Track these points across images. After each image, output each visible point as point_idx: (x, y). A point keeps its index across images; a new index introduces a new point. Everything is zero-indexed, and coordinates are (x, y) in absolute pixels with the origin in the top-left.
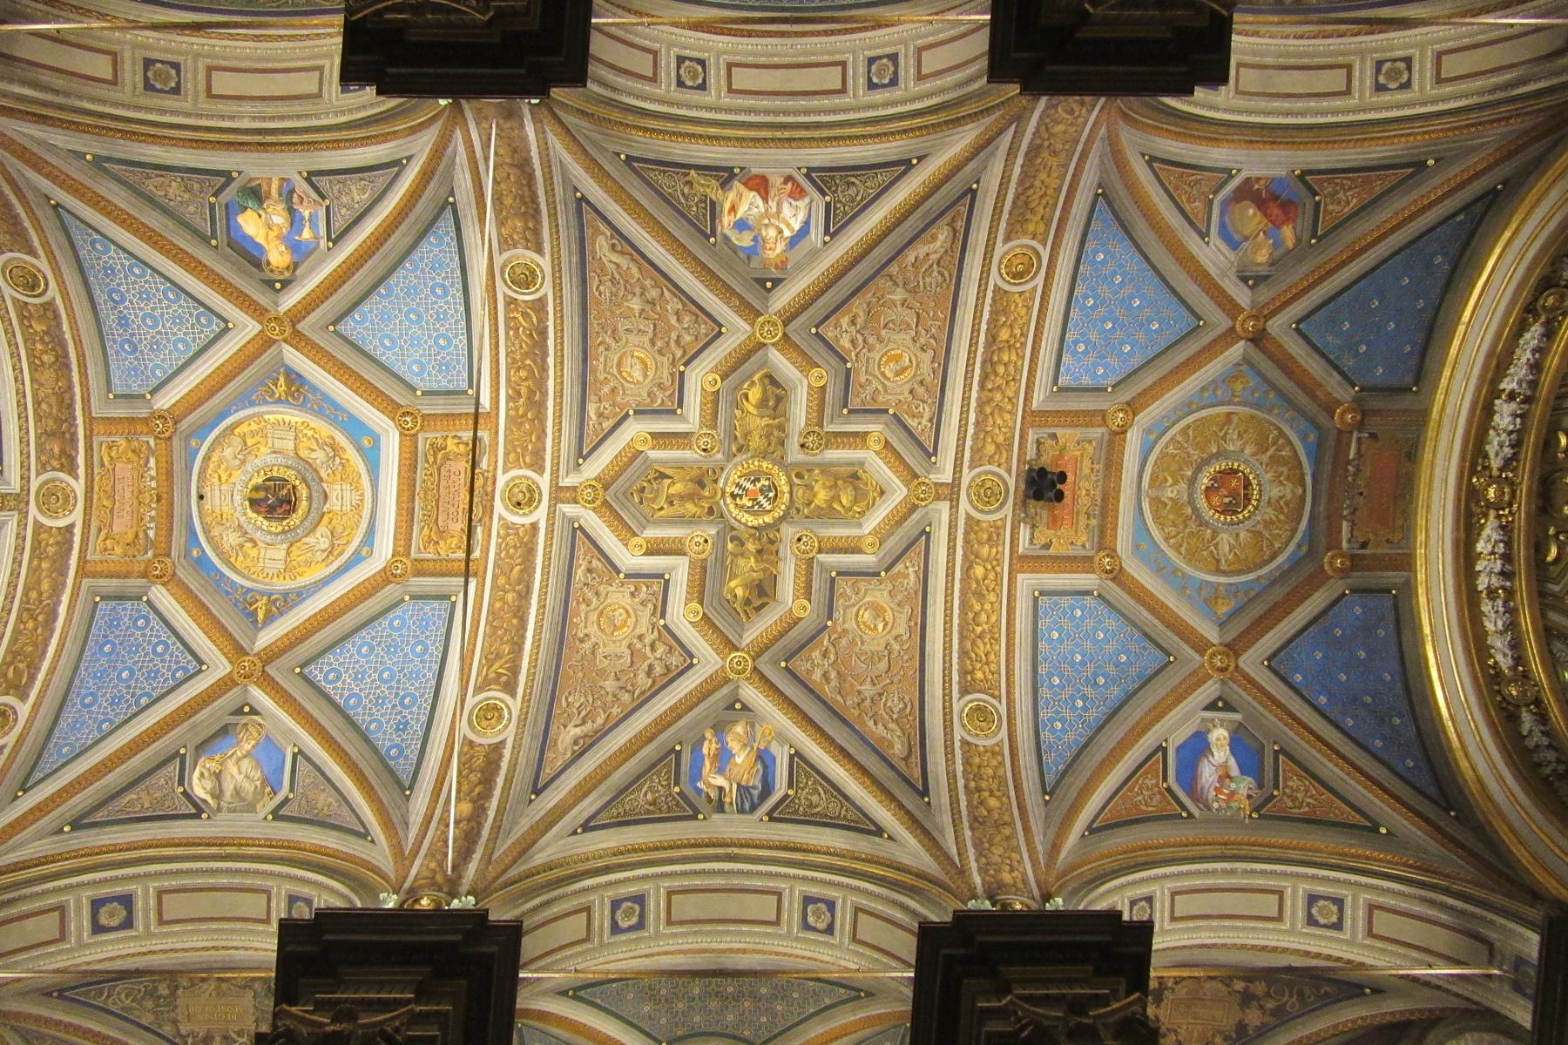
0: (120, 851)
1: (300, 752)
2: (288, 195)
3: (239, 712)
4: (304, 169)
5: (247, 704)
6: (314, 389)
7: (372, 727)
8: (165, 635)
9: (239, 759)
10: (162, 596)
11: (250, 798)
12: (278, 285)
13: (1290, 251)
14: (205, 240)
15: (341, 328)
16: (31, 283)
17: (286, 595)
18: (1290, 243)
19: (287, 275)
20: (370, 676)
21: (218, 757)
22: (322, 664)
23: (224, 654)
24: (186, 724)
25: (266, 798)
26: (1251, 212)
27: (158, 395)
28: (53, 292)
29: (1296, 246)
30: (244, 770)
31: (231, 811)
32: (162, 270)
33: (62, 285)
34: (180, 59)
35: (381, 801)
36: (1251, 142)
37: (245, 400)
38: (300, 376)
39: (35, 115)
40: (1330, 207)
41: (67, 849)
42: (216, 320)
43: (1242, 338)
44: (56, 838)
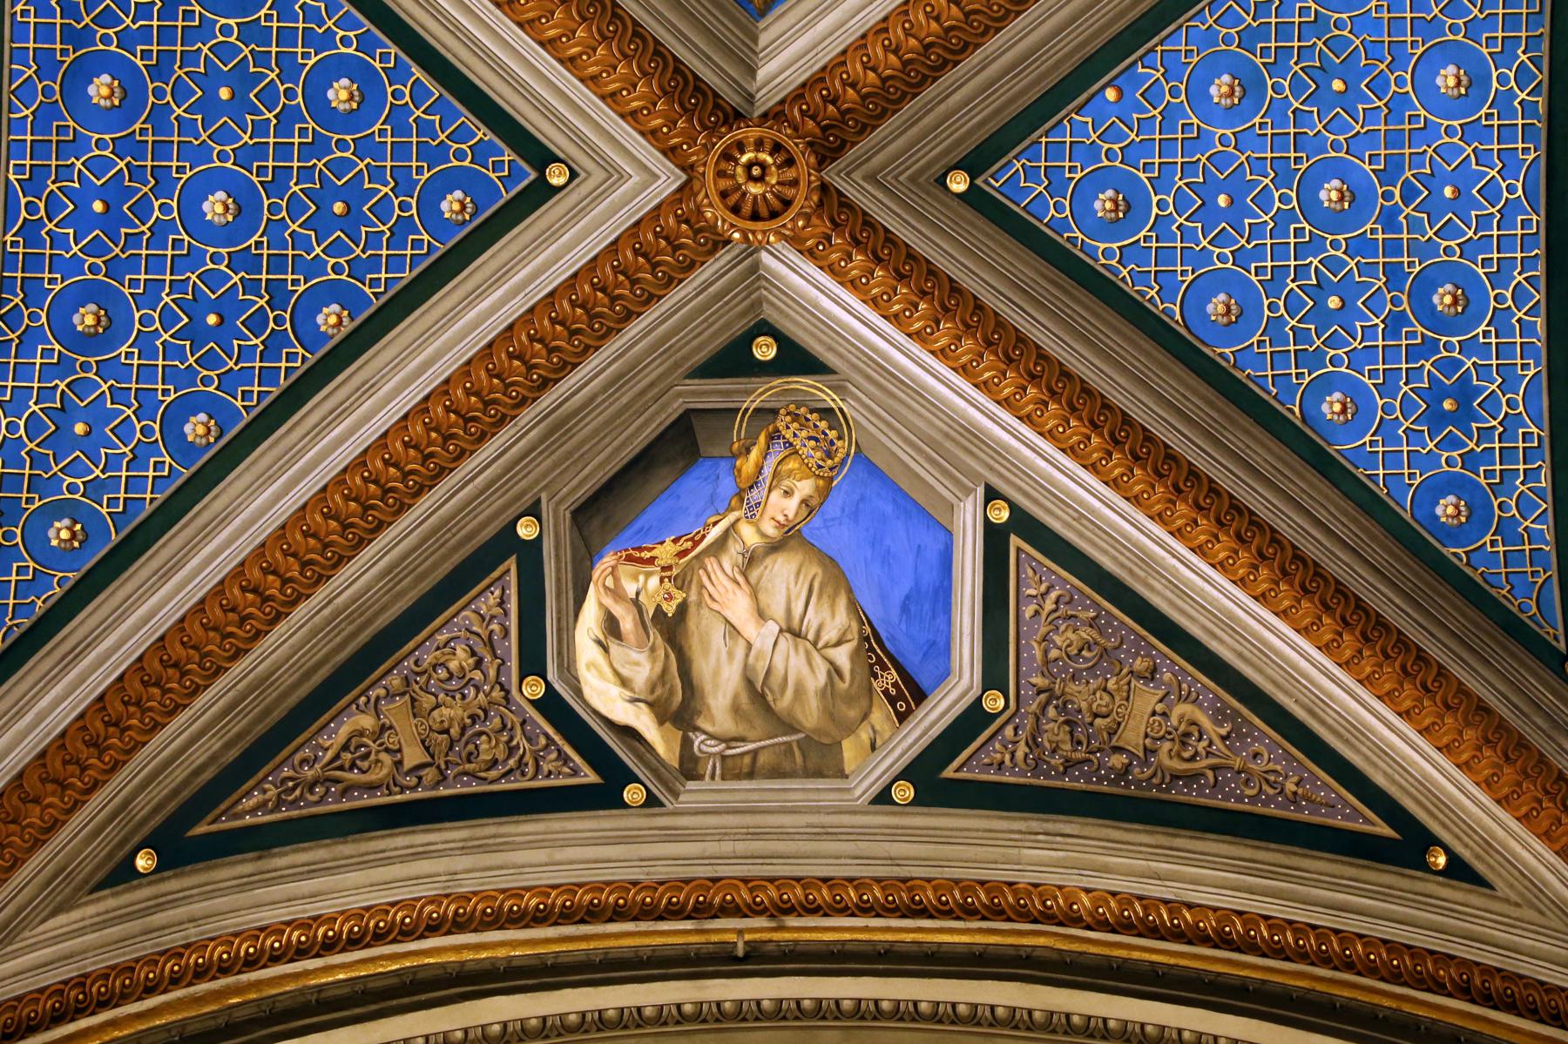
0: (329, 946)
1: (1023, 522)
5: (765, 328)
7: (1331, 406)
9: (751, 559)
11: (811, 715)
20: (1263, 200)
21: (666, 552)
22: (1055, 150)
23: (631, 116)
24: (528, 415)
25: (881, 716)
30: (777, 608)
31: (733, 770)
35: (1483, 709)
41: (147, 948)
44: (110, 902)
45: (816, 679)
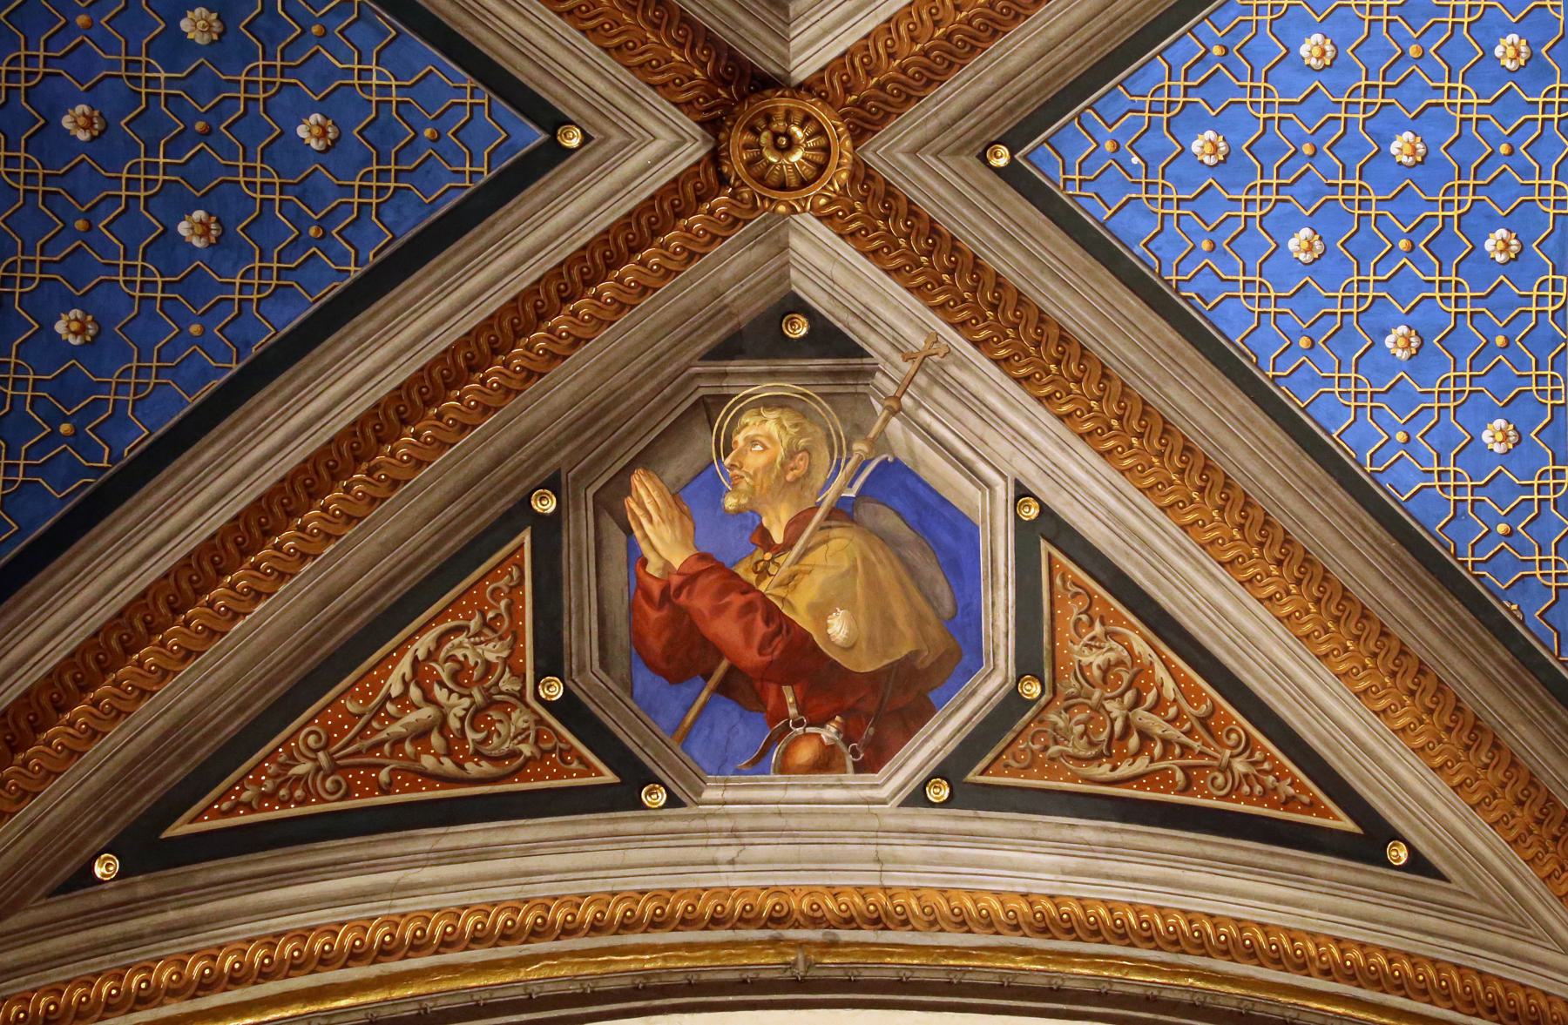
13: (644, 460)
18: (646, 493)
26: (839, 627)
29: (620, 485)
36: (877, 922)
40: (493, 652)
43: (807, 87)
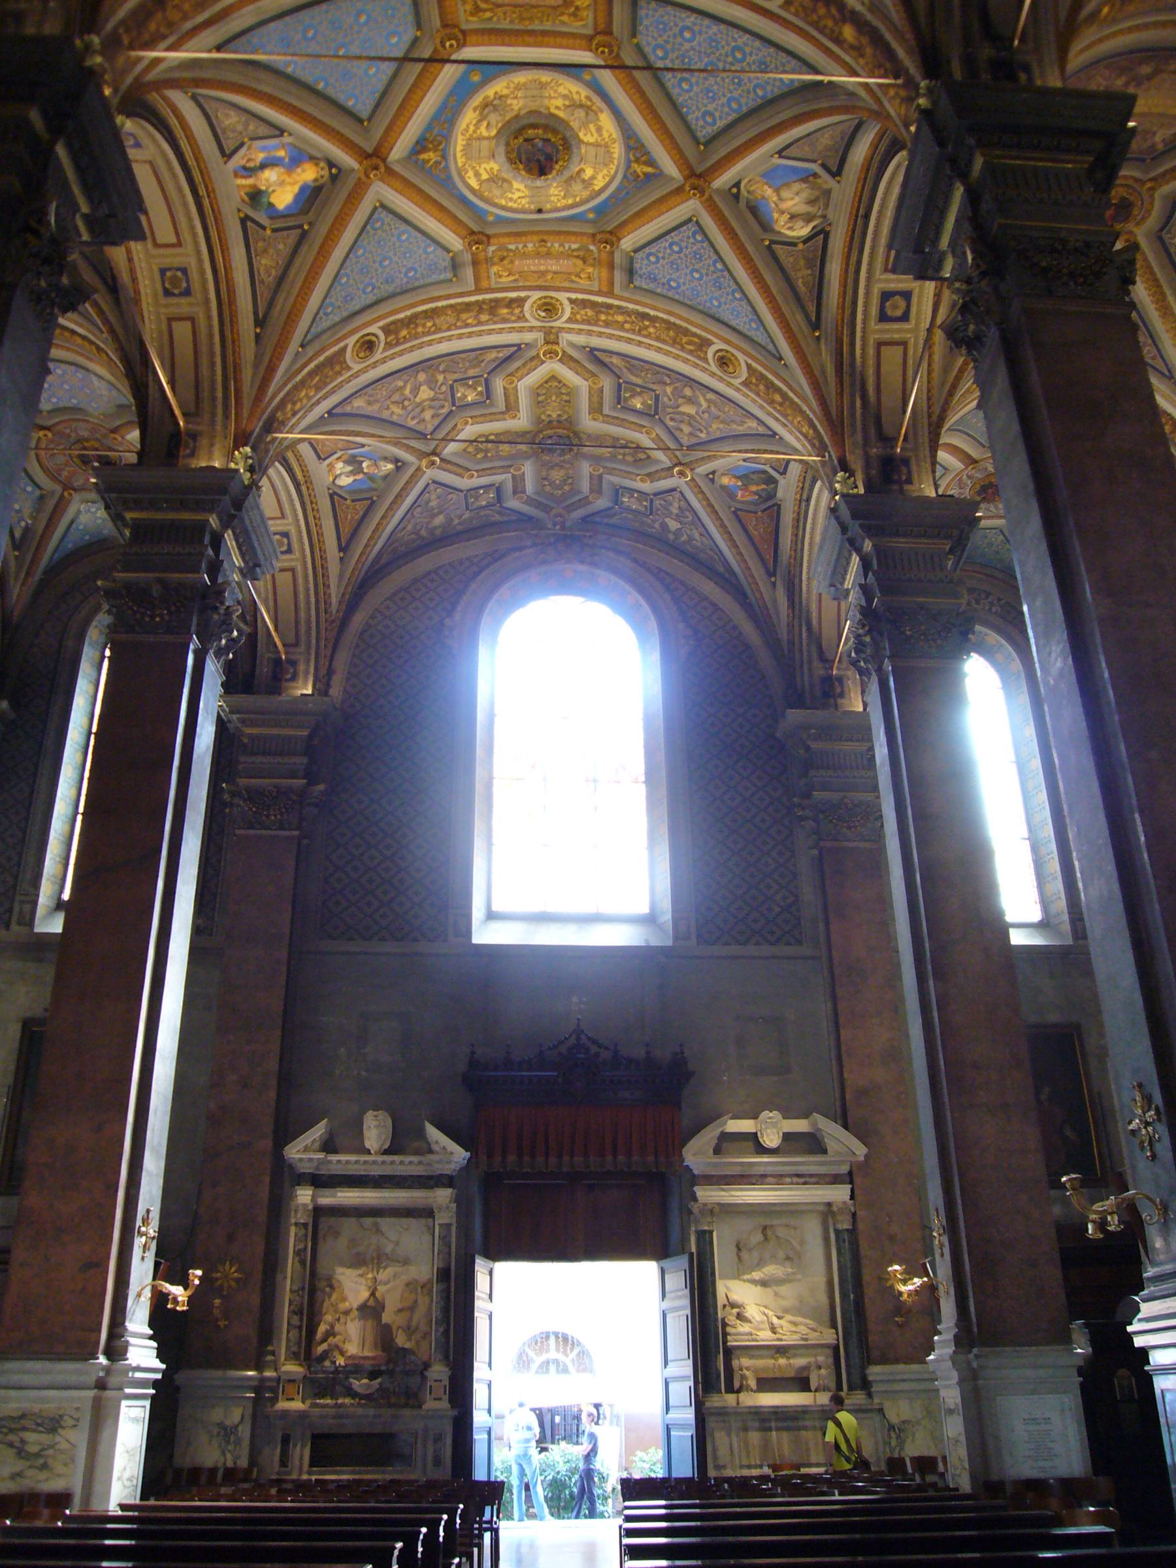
2: (249, 171)
3: (737, 197)
4: (221, 160)
5: (730, 189)
6: (429, 128)
7: (760, 93)
8: (663, 244)
9: (780, 199)
10: (627, 243)
11: (817, 193)
12: (334, 171)
14: (304, 235)
15: (364, 115)
16: (368, 345)
17: (629, 148)
19: (322, 164)
21: (776, 215)
25: (819, 181)
27: (451, 248)
28: (374, 329)
32: (340, 262)
33: (366, 325)
34: (155, 268)
37: (446, 182)
38: (417, 142)
39: (235, 372)
42: (375, 216)
45: (809, 191)
